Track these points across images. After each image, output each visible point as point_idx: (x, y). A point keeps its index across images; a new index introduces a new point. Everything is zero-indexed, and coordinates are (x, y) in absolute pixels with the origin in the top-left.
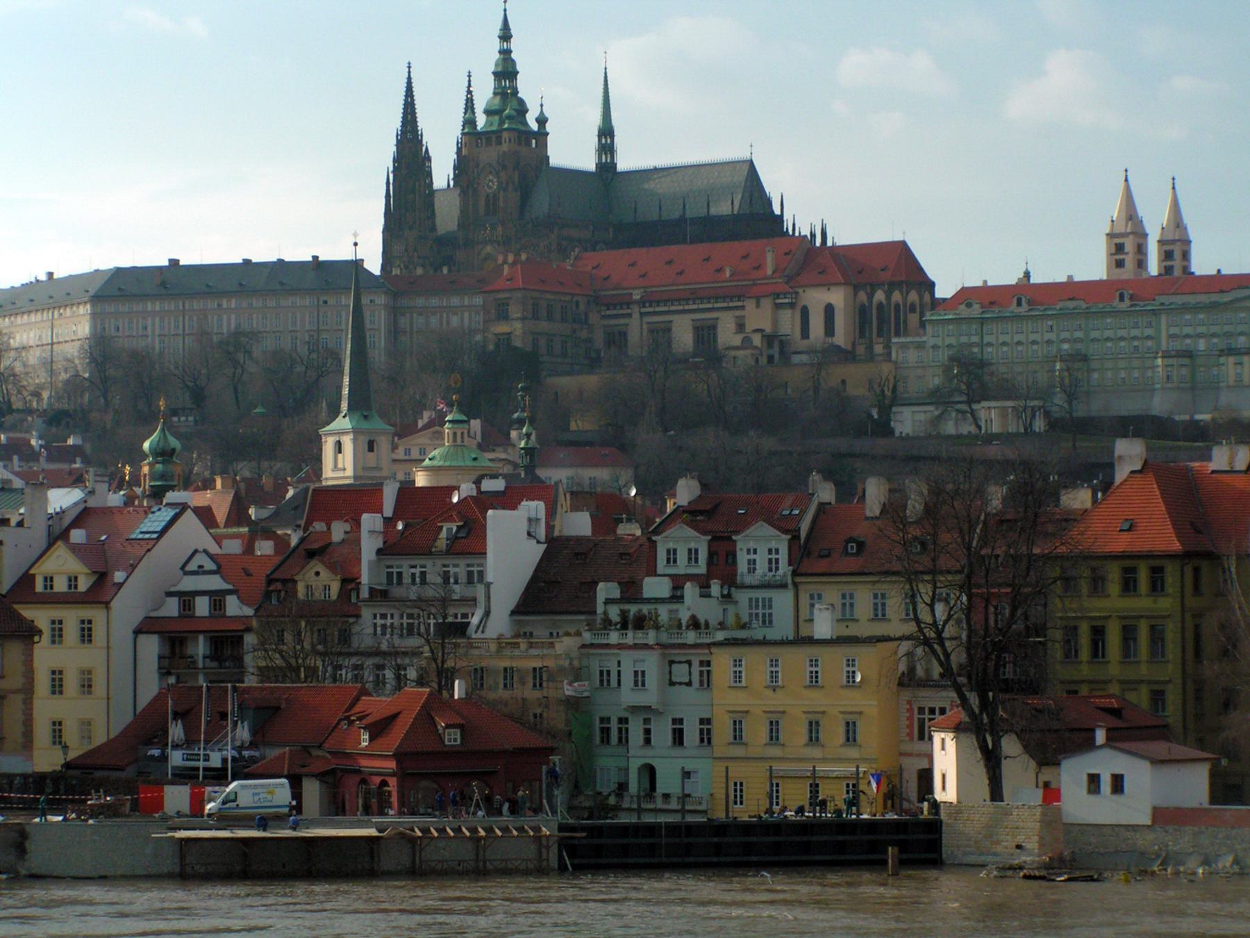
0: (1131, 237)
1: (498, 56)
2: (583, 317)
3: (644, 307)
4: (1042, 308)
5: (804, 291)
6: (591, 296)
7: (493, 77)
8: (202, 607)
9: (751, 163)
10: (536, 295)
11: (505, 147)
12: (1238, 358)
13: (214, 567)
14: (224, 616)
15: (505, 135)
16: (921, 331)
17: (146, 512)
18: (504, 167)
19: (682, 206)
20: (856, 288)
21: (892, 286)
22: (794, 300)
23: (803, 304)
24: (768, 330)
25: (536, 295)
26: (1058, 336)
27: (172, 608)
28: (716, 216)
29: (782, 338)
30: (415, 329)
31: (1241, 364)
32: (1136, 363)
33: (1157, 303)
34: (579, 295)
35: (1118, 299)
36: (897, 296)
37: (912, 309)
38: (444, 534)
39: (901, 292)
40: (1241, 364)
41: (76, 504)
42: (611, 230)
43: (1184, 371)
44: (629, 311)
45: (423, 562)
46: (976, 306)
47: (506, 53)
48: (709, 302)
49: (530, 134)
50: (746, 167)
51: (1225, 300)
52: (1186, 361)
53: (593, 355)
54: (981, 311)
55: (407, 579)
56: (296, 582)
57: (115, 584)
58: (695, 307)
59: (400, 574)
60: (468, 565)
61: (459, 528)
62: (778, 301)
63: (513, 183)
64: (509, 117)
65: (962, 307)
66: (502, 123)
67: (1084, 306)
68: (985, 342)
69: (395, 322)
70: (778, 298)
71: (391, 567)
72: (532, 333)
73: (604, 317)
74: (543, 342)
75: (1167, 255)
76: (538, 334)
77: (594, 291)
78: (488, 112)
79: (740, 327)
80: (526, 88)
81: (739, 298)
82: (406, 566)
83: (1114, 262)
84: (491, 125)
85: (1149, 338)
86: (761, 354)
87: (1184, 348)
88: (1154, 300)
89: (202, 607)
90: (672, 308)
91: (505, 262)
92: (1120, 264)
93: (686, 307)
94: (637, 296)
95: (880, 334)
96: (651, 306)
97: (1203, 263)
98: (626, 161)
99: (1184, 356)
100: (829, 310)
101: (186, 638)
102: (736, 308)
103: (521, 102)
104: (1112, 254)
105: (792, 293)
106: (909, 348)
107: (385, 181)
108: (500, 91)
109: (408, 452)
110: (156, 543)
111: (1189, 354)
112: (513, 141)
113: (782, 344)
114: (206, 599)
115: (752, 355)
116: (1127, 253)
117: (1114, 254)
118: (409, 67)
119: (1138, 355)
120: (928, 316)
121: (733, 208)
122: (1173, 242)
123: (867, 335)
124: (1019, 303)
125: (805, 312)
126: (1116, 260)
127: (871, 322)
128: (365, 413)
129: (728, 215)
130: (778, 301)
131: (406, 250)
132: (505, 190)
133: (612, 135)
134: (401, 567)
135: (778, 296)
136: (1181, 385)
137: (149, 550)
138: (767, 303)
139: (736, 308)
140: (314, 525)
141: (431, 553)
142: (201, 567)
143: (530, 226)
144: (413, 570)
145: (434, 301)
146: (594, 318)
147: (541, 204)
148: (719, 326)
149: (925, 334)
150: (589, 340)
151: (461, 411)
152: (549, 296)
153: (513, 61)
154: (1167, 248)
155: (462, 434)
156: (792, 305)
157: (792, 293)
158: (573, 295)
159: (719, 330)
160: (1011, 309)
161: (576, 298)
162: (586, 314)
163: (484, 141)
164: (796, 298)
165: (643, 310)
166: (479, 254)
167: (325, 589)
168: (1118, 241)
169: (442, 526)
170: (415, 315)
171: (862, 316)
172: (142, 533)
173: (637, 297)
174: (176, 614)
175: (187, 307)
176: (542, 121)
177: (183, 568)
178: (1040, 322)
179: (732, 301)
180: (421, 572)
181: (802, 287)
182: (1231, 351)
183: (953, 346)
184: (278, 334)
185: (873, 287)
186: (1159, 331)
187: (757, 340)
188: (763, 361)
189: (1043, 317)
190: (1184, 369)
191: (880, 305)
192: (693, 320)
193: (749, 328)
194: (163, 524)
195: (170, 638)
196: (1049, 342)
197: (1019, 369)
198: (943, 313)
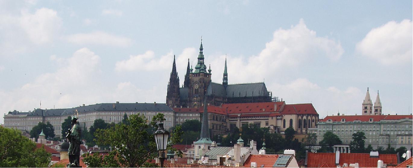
0: (369, 105)
1: (199, 54)
3: (241, 118)
4: (349, 122)
5: (284, 116)
7: (198, 59)
9: (264, 83)
10: (214, 114)
11: (201, 77)
12: (402, 137)
15: (201, 74)
16: (315, 127)
18: (201, 82)
19: (245, 94)
20: (298, 115)
21: (308, 115)
23: (284, 119)
24: (275, 125)
29: (278, 127)
30: (180, 122)
31: (403, 138)
34: (224, 115)
35: (370, 121)
36: (309, 118)
37: (313, 121)
39: (311, 117)
40: (403, 138)
42: (227, 99)
43: (387, 140)
44: (237, 119)
46: (332, 121)
47: (201, 53)
48: (259, 117)
49: (207, 74)
50: (262, 84)
51: (399, 122)
54: (332, 122)
58: (255, 119)
62: (277, 118)
63: (203, 86)
64: (202, 70)
65: (328, 121)
66: (200, 71)
67: (361, 122)
68: (334, 130)
69: (175, 120)
70: (277, 117)
72: (213, 124)
73: (230, 120)
74: (215, 126)
75: (376, 110)
78: (196, 68)
79: (267, 124)
80: (206, 62)
83: (364, 112)
84: (197, 71)
86: (273, 131)
88: (380, 121)
92: (366, 112)
93: (249, 119)
97: (385, 112)
98: (229, 83)
99: (387, 136)
100: (291, 121)
102: (266, 119)
103: (205, 66)
104: (364, 109)
105: (281, 116)
108: (200, 63)
109: (190, 152)
111: (389, 135)
113: (278, 129)
116: (368, 109)
118: (175, 56)
122: (378, 107)
123: (301, 127)
124: (343, 121)
125: (284, 121)
126: (365, 111)
127: (302, 125)
130: (277, 118)
131: (173, 103)
132: (201, 88)
135: (277, 116)
136: (386, 143)
138: (274, 118)
139: (266, 119)
140: (344, 164)
145: (185, 115)
146: (227, 121)
147: (210, 92)
149: (317, 128)
150: (226, 126)
152: (217, 115)
153: (203, 55)
154: (376, 108)
156: (281, 119)
158: (223, 114)
159: (261, 125)
160: (341, 122)
162: (225, 119)
163: (195, 75)
165: (241, 119)
166: (193, 104)
168: (366, 106)
170: (180, 118)
171: (299, 123)
173: (239, 116)
176: (210, 71)
178: (348, 126)
179: (265, 117)
181: (283, 114)
182: (398, 135)
183: (325, 131)
185: (303, 115)
186: (380, 129)
187: (272, 128)
188: (274, 133)
189: (350, 124)
190: (387, 139)
191: (305, 120)
192: (254, 122)
196: (351, 131)
197: (342, 137)
198: (322, 122)
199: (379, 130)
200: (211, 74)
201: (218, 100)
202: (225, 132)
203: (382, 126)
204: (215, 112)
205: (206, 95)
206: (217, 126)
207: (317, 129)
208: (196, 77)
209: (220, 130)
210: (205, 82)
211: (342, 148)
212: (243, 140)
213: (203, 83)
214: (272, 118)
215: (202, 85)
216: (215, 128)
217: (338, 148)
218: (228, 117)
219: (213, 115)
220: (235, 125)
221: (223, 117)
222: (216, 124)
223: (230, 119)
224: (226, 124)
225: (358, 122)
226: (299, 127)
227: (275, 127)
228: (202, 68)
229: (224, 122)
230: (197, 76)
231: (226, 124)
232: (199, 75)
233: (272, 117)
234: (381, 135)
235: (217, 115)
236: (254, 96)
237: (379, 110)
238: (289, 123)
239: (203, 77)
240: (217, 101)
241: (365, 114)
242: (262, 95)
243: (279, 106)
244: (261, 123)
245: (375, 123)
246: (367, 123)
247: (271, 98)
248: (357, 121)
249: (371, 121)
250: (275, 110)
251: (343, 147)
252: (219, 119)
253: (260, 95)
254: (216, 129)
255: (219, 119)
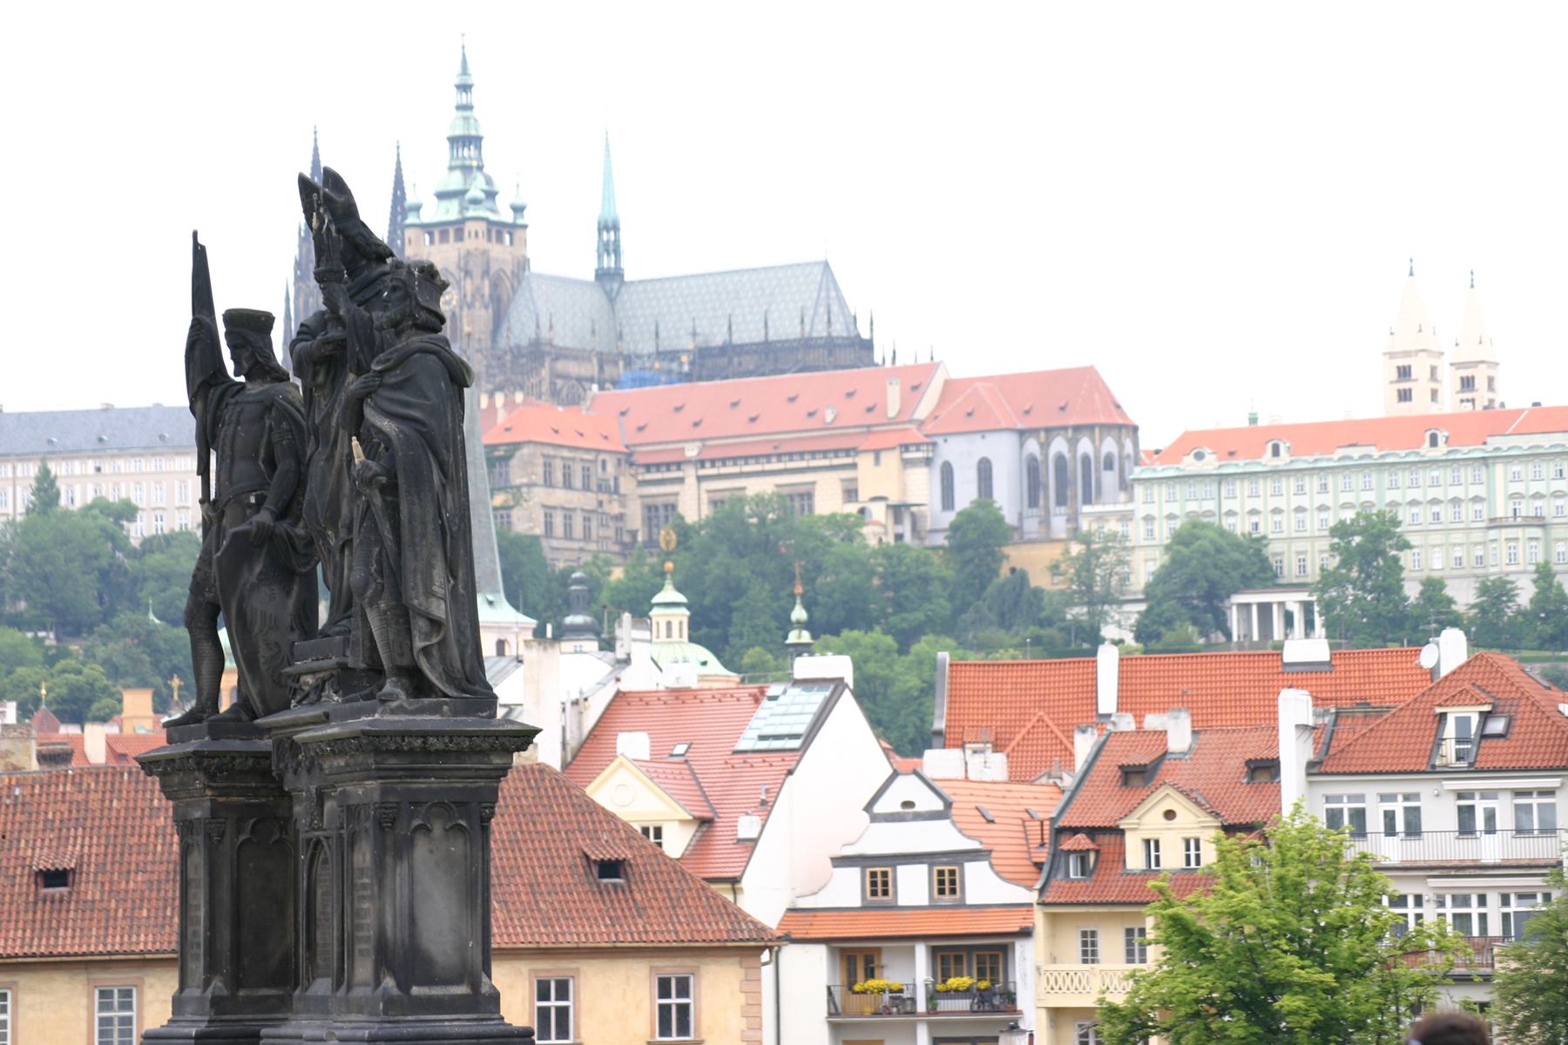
2: (612, 483)
3: (703, 466)
4: (1311, 459)
6: (620, 453)
7: (447, 144)
8: (913, 886)
9: (826, 265)
10: (551, 451)
11: (469, 244)
13: (938, 805)
14: (962, 905)
15: (470, 227)
16: (1122, 496)
17: (757, 701)
18: (468, 273)
19: (725, 328)
20: (1023, 434)
22: (931, 455)
24: (894, 499)
25: (551, 451)
26: (1336, 497)
27: (847, 889)
28: (779, 342)
29: (914, 509)
32: (1457, 537)
33: (1489, 447)
34: (606, 451)
36: (1085, 446)
37: (1109, 465)
38: (1450, 730)
39: (1093, 442)
41: (603, 684)
45: (1356, 790)
50: (818, 270)
52: (1537, 532)
53: (627, 538)
54: (1217, 464)
55: (1375, 822)
56: (1121, 832)
57: (739, 841)
59: (1359, 816)
60: (1461, 795)
61: (1485, 717)
62: (907, 456)
63: (482, 296)
64: (475, 202)
65: (1190, 459)
66: (463, 209)
68: (1224, 510)
71: (1339, 799)
72: (544, 506)
74: (558, 520)
76: (554, 508)
77: (627, 447)
79: (851, 494)
81: (848, 452)
82: (1374, 799)
85: (1476, 499)
86: (886, 533)
87: (1532, 514)
88: (1485, 443)
89: (913, 886)
90: (746, 469)
91: (492, 404)
94: (692, 451)
95: (1061, 500)
96: (713, 465)
97: (1514, 395)
100: (985, 471)
101: (879, 950)
103: (489, 181)
104: (1392, 382)
106: (1107, 521)
107: (284, 297)
108: (459, 163)
110: (802, 757)
112: (480, 235)
114: (922, 870)
115: (874, 534)
116: (1416, 380)
117: (1398, 381)
119: (1439, 527)
120: (1138, 472)
121: (803, 329)
123: (1042, 502)
125: (947, 473)
128: (491, 598)
129: (795, 340)
130: (907, 456)
132: (470, 306)
133: (615, 228)
134: (1361, 798)
137: (790, 772)
138: (891, 460)
141: (1433, 770)
142: (908, 804)
143: (508, 357)
144: (1389, 806)
146: (627, 485)
148: (816, 493)
150: (620, 517)
151: (679, 589)
152: (566, 453)
153: (476, 120)
155: (681, 623)
156: (928, 462)
157: (927, 444)
158: (599, 451)
161: (602, 457)
162: (616, 479)
164: (933, 451)
165: (702, 472)
167: (1188, 849)
169: (1443, 716)
171: (1033, 471)
172: (762, 738)
174: (924, 900)
175: (19, 473)
176: (518, 210)
177: (868, 808)
180: (1407, 810)
184: (159, 513)
187: (878, 512)
188: (890, 540)
191: (1060, 459)
193: (864, 495)
194: (808, 719)
195: (842, 950)
196: (1322, 508)
199: (1483, 494)
200: (525, 227)
201: (573, 368)
202: (616, 548)
203: (1499, 469)
204: (557, 440)
205: (502, 343)
206: (568, 518)
207: (1129, 507)
208: (445, 247)
209: (587, 537)
210: (493, 270)
211: (1275, 608)
212: (682, 598)
213: (483, 277)
214: (877, 461)
215: (478, 290)
216: (559, 530)
217: (1254, 609)
218: (631, 464)
219: (544, 456)
220: (674, 507)
221: (604, 468)
222: (563, 508)
223: (640, 478)
224: (623, 505)
225: (1362, 457)
226: (1033, 502)
227: (898, 511)
228: (476, 192)
229: (608, 491)
230: (444, 237)
231: (623, 505)
232: (459, 237)
233: (877, 453)
234: (1495, 524)
235: (566, 453)
236: (772, 336)
237: (1481, 383)
238: (973, 475)
239: (482, 243)
240: (565, 377)
241: (1404, 409)
242: (820, 331)
243: (915, 388)
244: (817, 487)
245: (1459, 456)
246: (1411, 459)
247: (868, 346)
248: (1356, 453)
249: (1434, 441)
250: (892, 413)
251: (1281, 604)
252: (577, 481)
253: (807, 328)
254: (568, 536)
255: (577, 481)
